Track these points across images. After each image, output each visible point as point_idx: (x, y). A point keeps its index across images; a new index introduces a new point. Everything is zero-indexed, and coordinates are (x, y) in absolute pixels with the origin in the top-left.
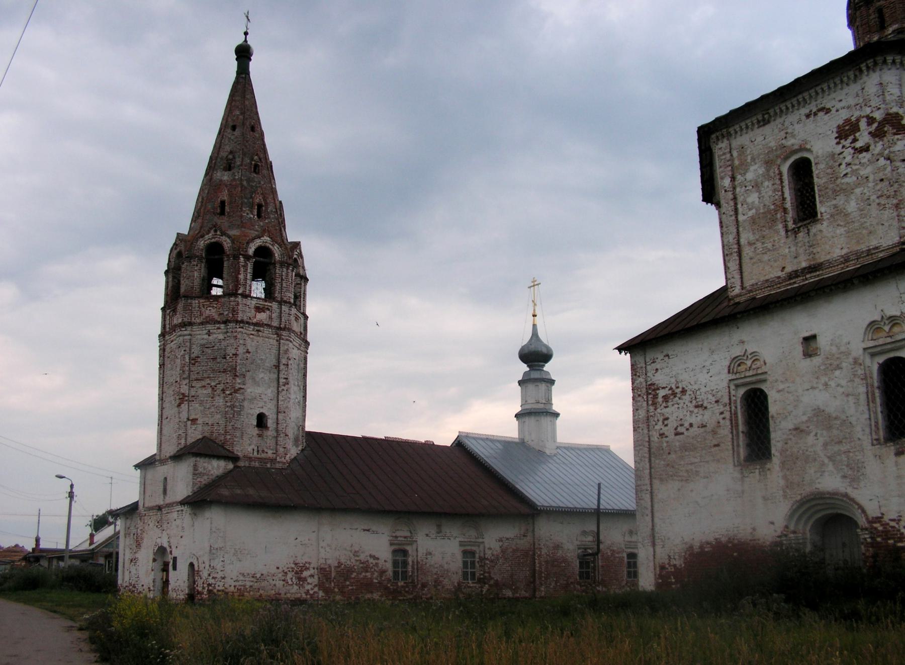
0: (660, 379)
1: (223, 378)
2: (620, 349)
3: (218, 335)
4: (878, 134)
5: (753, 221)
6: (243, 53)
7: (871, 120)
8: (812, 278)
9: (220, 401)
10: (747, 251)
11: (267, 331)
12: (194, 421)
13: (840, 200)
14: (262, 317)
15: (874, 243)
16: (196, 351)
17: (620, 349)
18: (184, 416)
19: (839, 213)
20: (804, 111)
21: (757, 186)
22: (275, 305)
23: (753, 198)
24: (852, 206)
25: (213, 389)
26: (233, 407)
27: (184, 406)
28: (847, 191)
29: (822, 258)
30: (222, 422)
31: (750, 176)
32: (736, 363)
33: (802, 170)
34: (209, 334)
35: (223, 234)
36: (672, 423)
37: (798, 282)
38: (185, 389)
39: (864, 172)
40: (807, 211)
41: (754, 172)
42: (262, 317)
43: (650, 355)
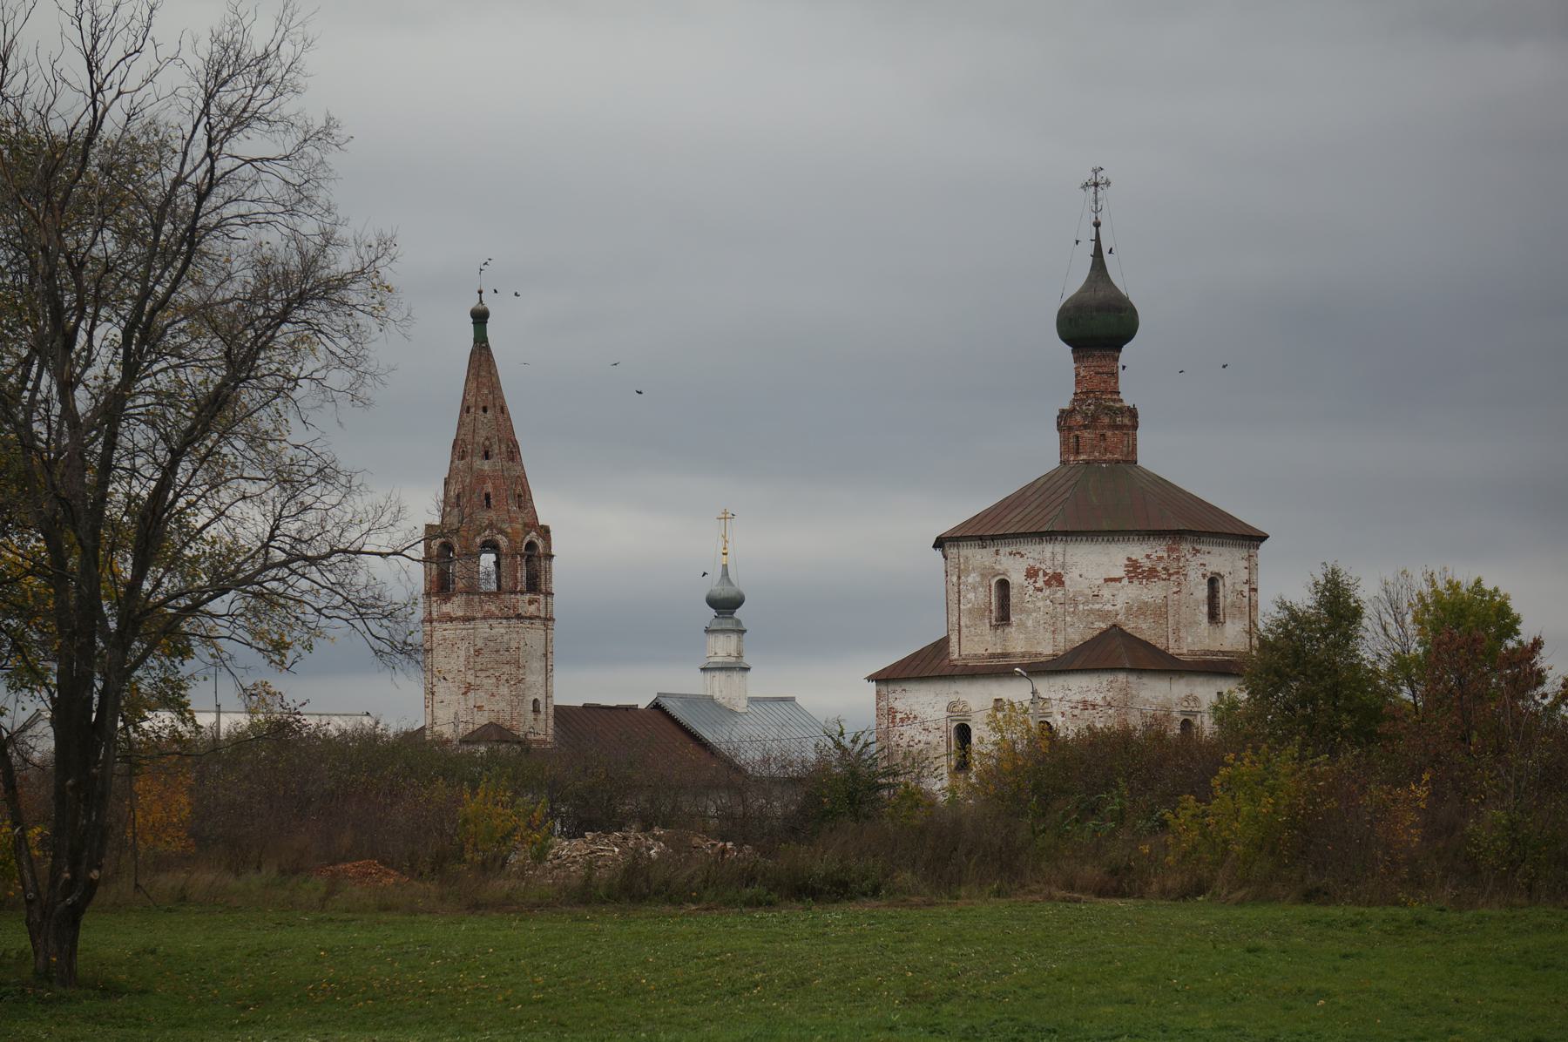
0: (898, 705)
1: (506, 668)
2: (870, 679)
3: (500, 629)
4: (1047, 583)
5: (970, 611)
6: (480, 318)
7: (1045, 574)
8: (1003, 662)
9: (504, 690)
10: (964, 630)
11: (538, 623)
12: (480, 708)
13: (1023, 617)
14: (532, 609)
15: (1039, 650)
16: (480, 644)
17: (870, 679)
18: (471, 703)
19: (1022, 624)
20: (1008, 550)
21: (974, 588)
22: (541, 597)
23: (971, 596)
24: (1030, 623)
25: (498, 679)
26: (517, 696)
27: (471, 695)
28: (1029, 612)
29: (1010, 650)
30: (508, 709)
31: (970, 580)
32: (951, 707)
33: (1004, 585)
34: (491, 627)
35: (501, 532)
36: (906, 738)
37: (995, 662)
38: (470, 679)
39: (1040, 604)
40: (1004, 618)
41: (973, 578)
42: (532, 609)
43: (891, 687)
